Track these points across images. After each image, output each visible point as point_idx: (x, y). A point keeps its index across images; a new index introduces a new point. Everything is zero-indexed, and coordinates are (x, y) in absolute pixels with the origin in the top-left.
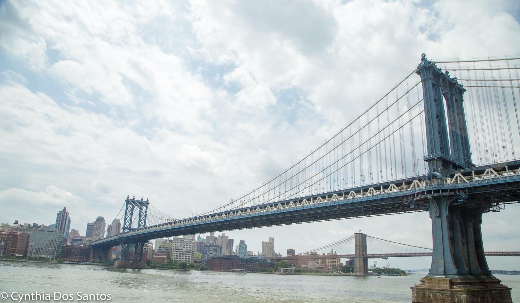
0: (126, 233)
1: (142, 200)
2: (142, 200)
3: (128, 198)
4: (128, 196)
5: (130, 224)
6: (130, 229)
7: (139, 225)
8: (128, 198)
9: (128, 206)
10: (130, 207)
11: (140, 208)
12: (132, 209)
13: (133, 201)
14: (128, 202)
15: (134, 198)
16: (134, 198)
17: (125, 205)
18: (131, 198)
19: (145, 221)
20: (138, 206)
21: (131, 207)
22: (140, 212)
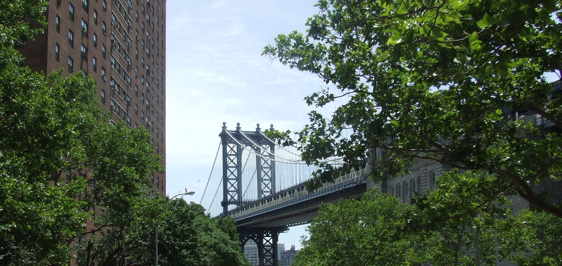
0: (233, 211)
1: (258, 129)
2: (258, 129)
3: (224, 127)
4: (224, 124)
5: (239, 191)
6: (239, 202)
7: (260, 191)
8: (224, 127)
9: (228, 149)
10: (232, 149)
11: (258, 150)
12: (239, 155)
13: (237, 134)
14: (225, 137)
15: (238, 128)
16: (238, 128)
17: (221, 146)
18: (232, 127)
19: (272, 179)
20: (251, 145)
21: (235, 149)
22: (258, 159)
